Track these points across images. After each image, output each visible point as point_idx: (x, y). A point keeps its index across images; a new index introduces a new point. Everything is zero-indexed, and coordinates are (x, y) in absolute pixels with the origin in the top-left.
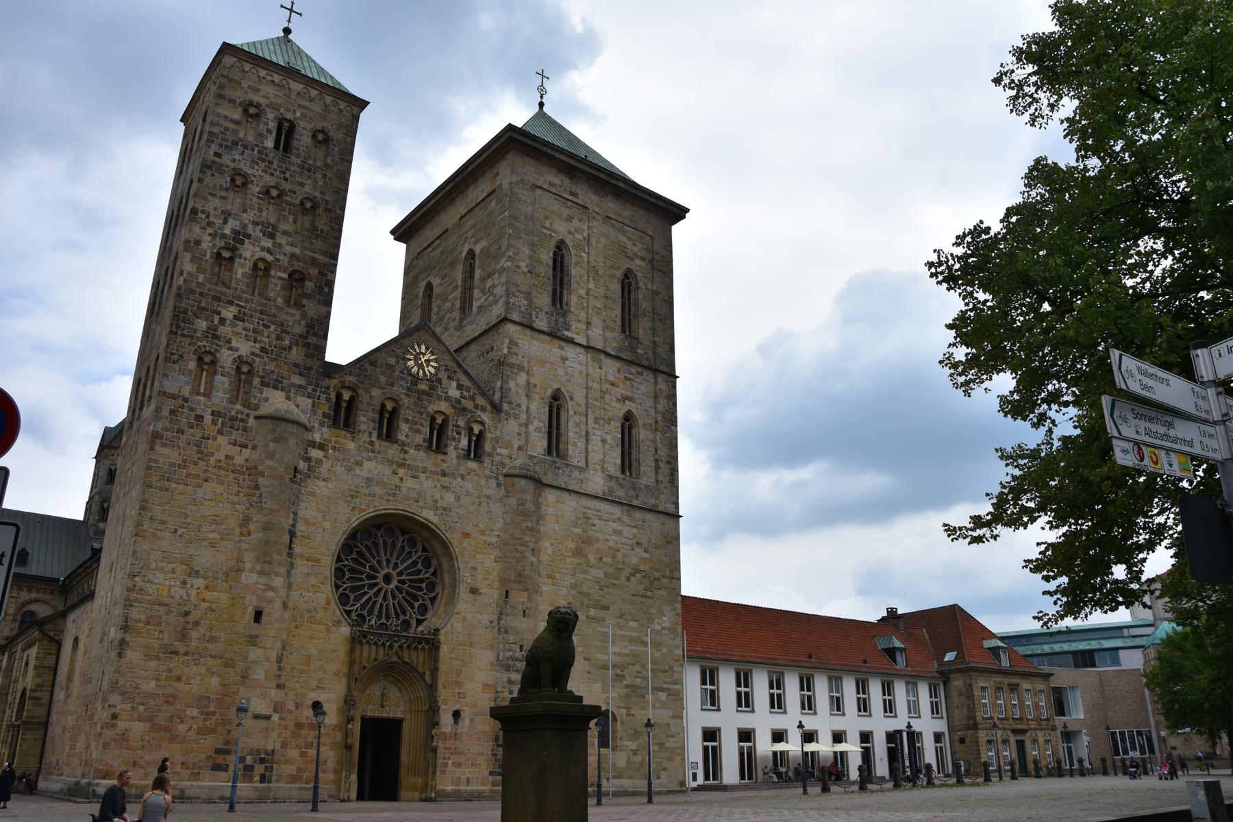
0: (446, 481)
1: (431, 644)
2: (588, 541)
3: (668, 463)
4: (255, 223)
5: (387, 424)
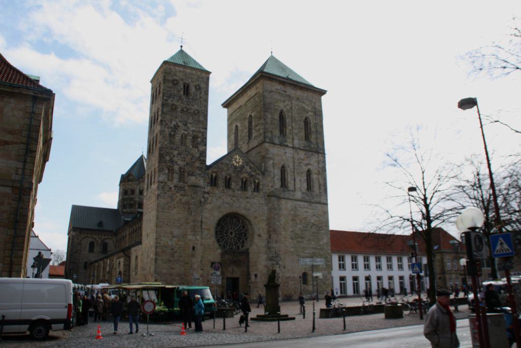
0: (248, 200)
1: (247, 253)
2: (296, 216)
3: (324, 186)
4: (180, 122)
5: (228, 184)
